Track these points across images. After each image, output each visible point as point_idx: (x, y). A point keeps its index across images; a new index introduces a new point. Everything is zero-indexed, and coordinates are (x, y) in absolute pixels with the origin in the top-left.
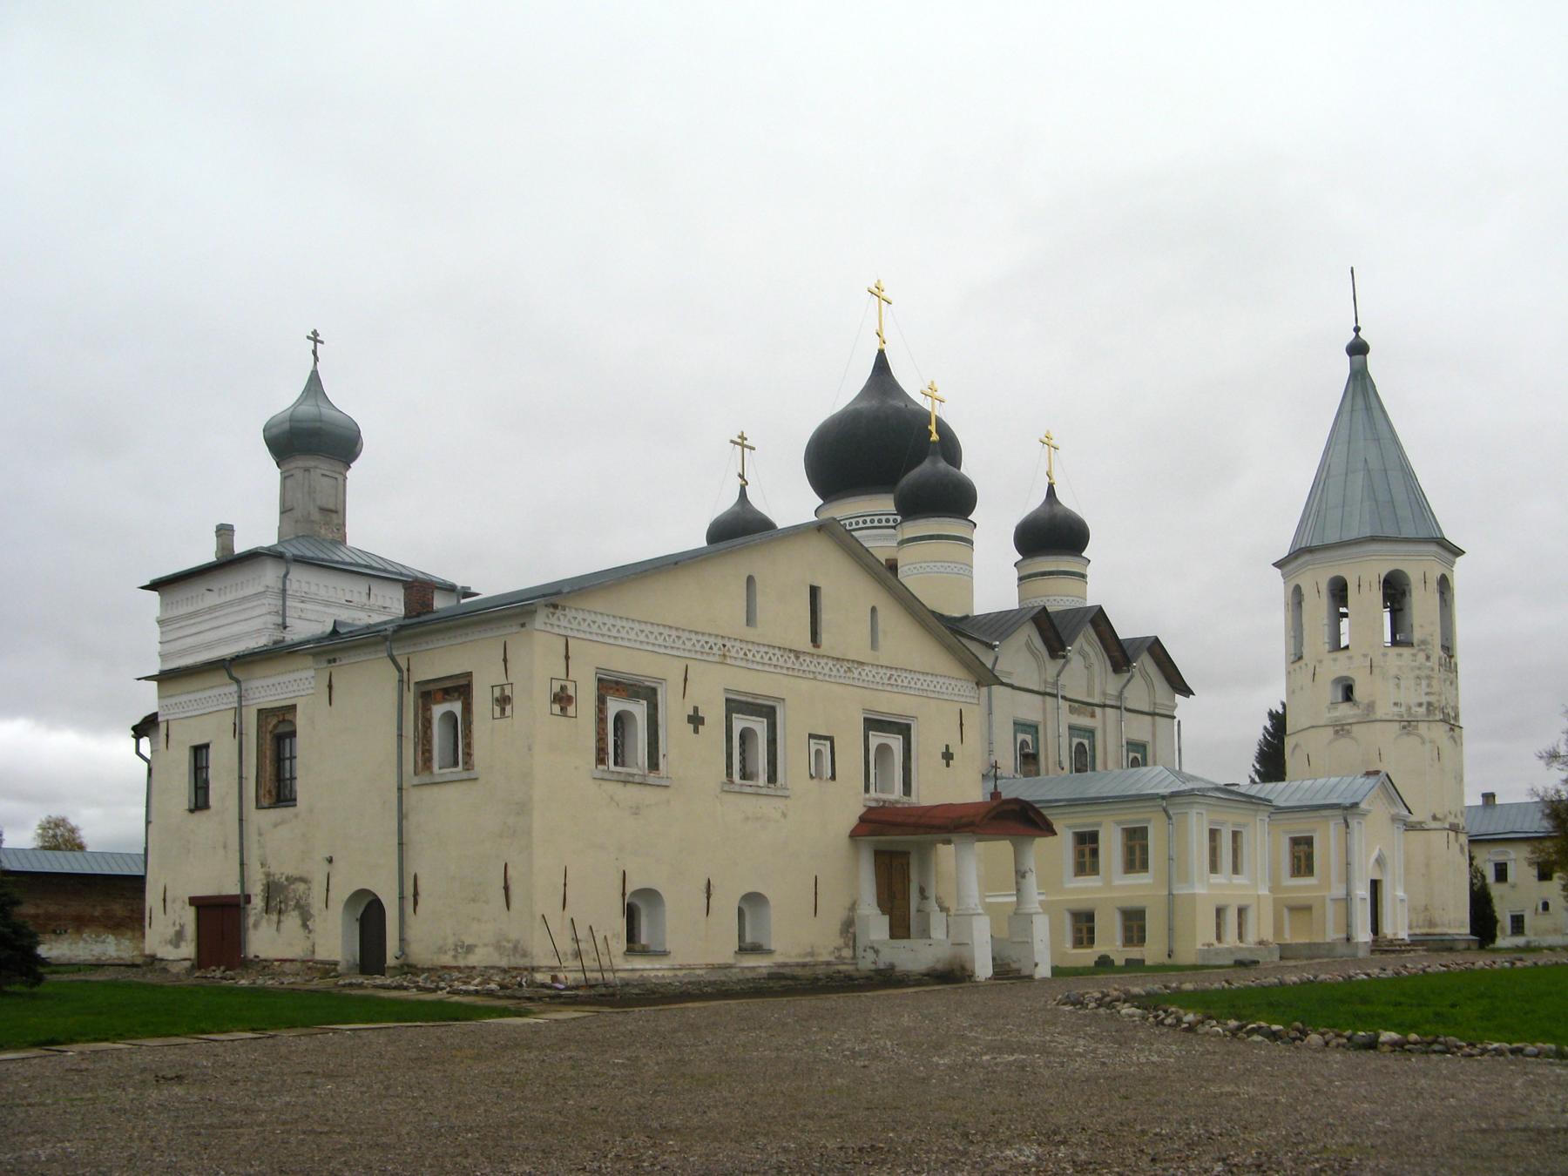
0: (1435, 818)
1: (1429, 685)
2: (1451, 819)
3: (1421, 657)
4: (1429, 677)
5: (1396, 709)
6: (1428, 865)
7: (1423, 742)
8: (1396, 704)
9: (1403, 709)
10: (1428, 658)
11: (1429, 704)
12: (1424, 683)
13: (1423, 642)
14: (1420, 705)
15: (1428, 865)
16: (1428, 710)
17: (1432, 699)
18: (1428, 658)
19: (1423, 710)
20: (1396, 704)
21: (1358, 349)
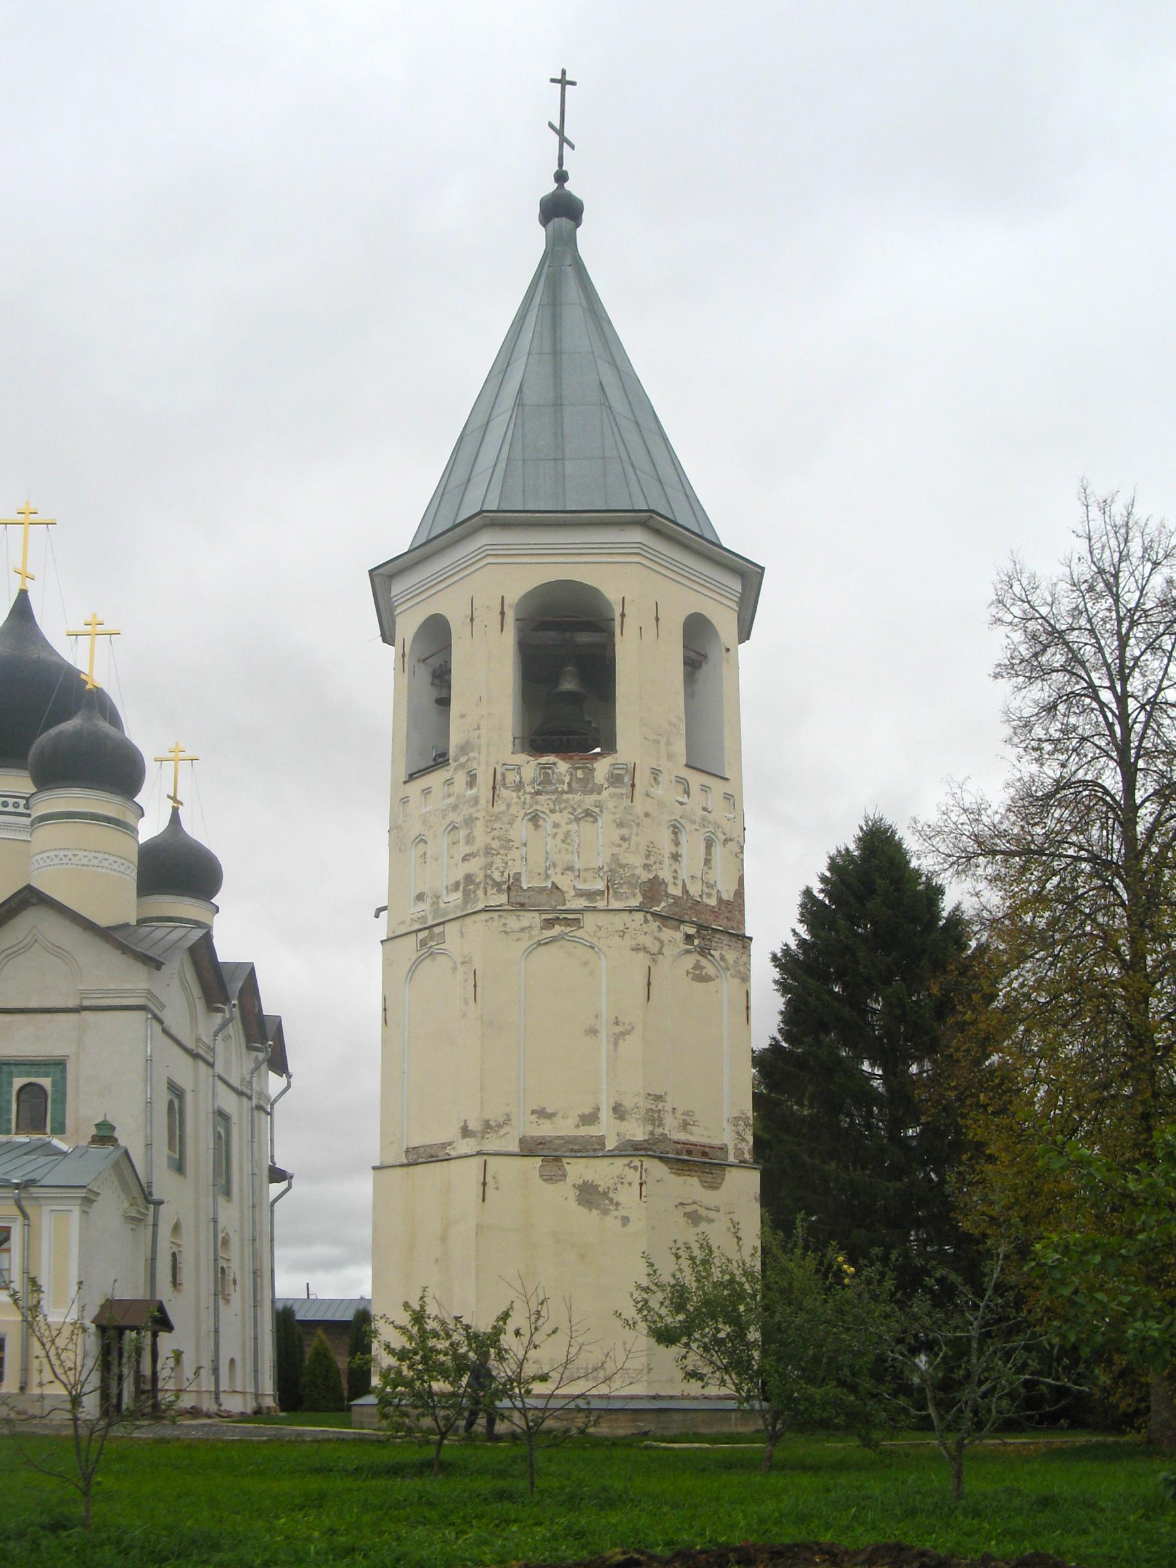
0: (466, 1132)
1: (470, 840)
2: (564, 1127)
3: (461, 778)
4: (470, 821)
5: (422, 906)
6: (444, 1239)
7: (454, 969)
8: (420, 897)
9: (426, 906)
10: (472, 781)
11: (469, 878)
12: (462, 833)
13: (465, 748)
14: (456, 886)
15: (444, 1239)
16: (466, 894)
17: (475, 866)
18: (472, 781)
19: (459, 895)
20: (420, 897)
21: (561, 210)
